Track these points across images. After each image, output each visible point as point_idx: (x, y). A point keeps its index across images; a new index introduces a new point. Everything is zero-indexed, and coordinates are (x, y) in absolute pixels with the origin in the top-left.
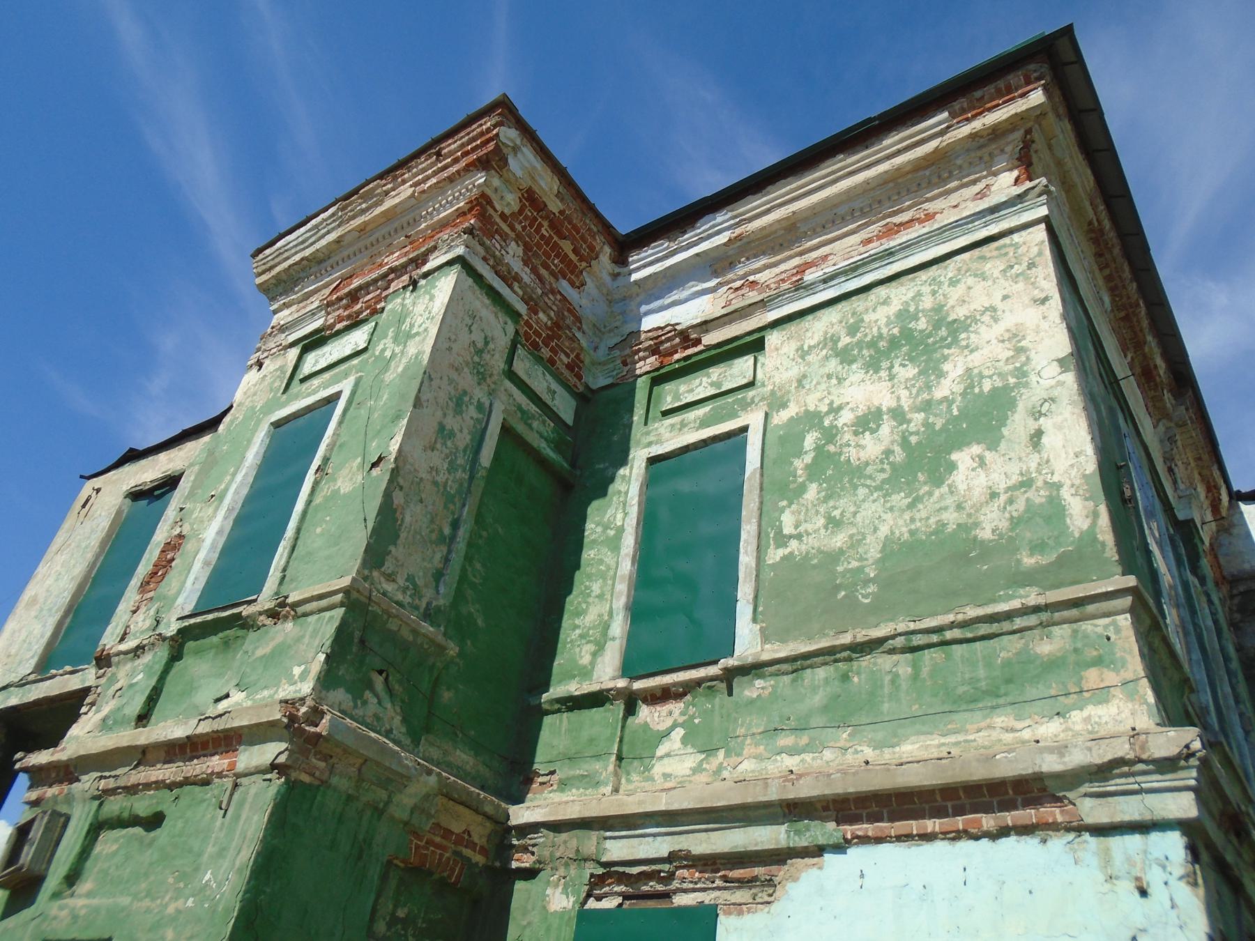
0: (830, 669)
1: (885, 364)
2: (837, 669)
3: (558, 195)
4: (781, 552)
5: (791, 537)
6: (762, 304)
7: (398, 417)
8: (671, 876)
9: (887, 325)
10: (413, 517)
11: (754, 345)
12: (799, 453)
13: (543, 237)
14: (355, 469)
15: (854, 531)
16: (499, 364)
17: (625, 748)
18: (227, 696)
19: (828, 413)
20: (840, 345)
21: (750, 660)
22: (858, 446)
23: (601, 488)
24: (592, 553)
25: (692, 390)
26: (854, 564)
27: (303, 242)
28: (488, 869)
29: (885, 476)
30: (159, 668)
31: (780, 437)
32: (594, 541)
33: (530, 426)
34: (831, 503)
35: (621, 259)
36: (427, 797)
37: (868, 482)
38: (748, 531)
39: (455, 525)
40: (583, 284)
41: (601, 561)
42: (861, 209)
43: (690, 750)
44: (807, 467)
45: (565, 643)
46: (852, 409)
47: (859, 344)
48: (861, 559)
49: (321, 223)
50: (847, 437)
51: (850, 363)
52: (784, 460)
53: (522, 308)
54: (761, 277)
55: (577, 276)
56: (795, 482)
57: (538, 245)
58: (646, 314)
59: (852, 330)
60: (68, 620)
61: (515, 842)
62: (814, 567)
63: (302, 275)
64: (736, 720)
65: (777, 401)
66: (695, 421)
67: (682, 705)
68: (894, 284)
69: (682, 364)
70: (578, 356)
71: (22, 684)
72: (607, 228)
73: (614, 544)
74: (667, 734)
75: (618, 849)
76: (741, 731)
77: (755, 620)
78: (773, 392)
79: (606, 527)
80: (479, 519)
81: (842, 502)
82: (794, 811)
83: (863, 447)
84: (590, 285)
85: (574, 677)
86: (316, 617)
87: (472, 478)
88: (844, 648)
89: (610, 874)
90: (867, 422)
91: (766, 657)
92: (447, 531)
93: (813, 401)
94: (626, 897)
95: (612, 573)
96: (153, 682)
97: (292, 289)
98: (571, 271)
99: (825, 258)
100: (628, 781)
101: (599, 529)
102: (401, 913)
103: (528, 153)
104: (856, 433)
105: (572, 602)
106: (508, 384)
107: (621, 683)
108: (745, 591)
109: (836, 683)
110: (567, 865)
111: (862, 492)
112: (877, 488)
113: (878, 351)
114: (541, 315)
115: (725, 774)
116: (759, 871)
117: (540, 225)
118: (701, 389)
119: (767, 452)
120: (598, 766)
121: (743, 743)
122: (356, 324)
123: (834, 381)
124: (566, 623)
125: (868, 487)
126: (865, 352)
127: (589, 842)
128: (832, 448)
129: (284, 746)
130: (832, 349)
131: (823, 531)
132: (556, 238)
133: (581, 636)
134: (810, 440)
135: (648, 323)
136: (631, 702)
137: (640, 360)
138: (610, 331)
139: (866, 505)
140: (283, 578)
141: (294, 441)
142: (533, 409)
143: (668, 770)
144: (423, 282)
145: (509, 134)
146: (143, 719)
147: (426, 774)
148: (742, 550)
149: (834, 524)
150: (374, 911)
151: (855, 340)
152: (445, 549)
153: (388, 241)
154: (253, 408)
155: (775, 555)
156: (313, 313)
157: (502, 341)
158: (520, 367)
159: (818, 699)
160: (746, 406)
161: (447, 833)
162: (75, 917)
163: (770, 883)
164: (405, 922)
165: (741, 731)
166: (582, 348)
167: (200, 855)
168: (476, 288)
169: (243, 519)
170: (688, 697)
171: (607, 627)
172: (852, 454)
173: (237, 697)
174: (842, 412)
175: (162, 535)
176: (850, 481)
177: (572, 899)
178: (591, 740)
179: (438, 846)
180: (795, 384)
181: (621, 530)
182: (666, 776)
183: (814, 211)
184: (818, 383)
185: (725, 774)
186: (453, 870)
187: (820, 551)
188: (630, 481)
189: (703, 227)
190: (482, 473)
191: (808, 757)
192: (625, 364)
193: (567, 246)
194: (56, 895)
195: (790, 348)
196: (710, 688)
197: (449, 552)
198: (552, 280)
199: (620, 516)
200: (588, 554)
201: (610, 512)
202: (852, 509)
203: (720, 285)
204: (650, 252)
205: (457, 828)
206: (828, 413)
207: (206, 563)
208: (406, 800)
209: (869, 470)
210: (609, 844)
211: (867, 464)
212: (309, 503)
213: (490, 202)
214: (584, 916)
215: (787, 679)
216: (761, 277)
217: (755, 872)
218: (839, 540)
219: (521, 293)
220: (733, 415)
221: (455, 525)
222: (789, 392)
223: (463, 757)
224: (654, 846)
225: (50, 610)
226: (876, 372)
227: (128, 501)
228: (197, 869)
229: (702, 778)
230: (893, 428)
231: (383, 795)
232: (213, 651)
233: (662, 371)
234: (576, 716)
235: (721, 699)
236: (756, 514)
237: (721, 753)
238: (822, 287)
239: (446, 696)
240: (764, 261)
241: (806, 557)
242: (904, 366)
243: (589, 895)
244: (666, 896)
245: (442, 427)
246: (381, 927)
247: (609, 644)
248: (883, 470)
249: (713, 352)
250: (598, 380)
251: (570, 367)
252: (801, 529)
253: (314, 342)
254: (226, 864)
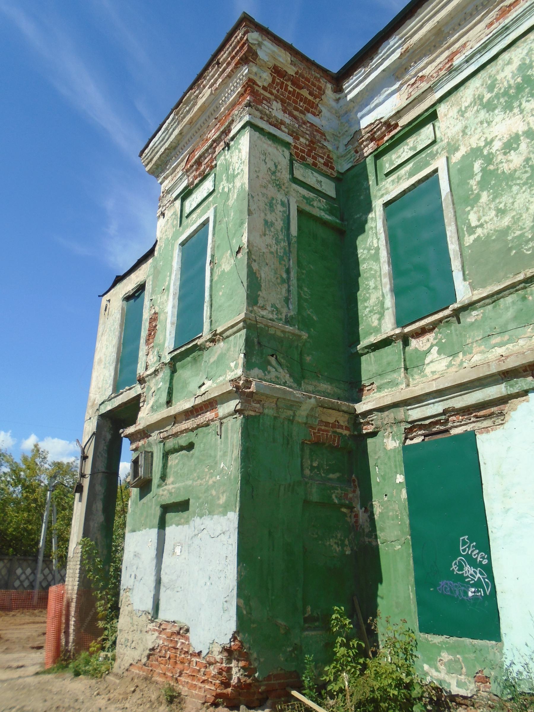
0: (514, 296)
1: (516, 104)
2: (518, 295)
3: (292, 63)
4: (472, 237)
5: (477, 227)
6: (431, 90)
7: (242, 223)
8: (447, 421)
9: (513, 77)
10: (265, 274)
11: (431, 116)
12: (472, 176)
13: (290, 92)
14: (229, 257)
15: (514, 213)
16: (286, 176)
17: (408, 363)
18: (204, 384)
19: (485, 146)
20: (485, 100)
21: (466, 302)
22: (508, 161)
23: (361, 229)
24: (365, 266)
25: (400, 156)
26: (518, 233)
27: (162, 140)
28: (352, 436)
29: (528, 175)
30: (168, 378)
31: (459, 170)
32: (364, 259)
33: (313, 205)
34: (497, 201)
35: (339, 89)
36: (312, 409)
37: (518, 182)
38: (450, 230)
39: (288, 272)
40: (320, 112)
41: (371, 269)
42: (482, 4)
43: (443, 356)
44: (479, 183)
45: (362, 317)
46: (500, 139)
47: (497, 96)
48: (522, 229)
49: (168, 126)
50: (500, 157)
51: (493, 110)
52: (464, 182)
53: (289, 139)
54: (426, 72)
55: (316, 108)
56: (472, 194)
57: (289, 98)
58: (362, 117)
59: (491, 88)
60: (119, 366)
61: (362, 421)
62: (494, 240)
63: (168, 159)
64: (465, 336)
65: (453, 148)
66: (405, 174)
67: (434, 334)
68: (513, 48)
69: (390, 142)
70: (328, 156)
71: (110, 399)
72: (325, 72)
73: (376, 257)
74: (429, 351)
75: (416, 413)
76: (469, 341)
77: (465, 279)
78: (448, 143)
79: (369, 250)
80: (299, 264)
81: (504, 199)
82: (507, 375)
83: (511, 161)
85: (371, 333)
86: (233, 337)
87: (289, 244)
88: (520, 282)
89: (414, 426)
90: (511, 144)
91: (475, 298)
92: (285, 276)
93: (475, 141)
94: (425, 436)
95: (378, 274)
96: (167, 385)
97: (166, 168)
98: (312, 107)
99: (464, 46)
100: (413, 379)
101: (365, 252)
102: (315, 464)
103: (268, 45)
104: (505, 154)
105: (361, 294)
106: (294, 186)
107: (398, 331)
108: (456, 265)
109: (519, 303)
110: (391, 426)
111: (515, 189)
112: (524, 184)
113: (510, 96)
114: (302, 140)
115: (465, 365)
116: (493, 409)
117: (287, 86)
118: (404, 154)
119: (452, 181)
120: (395, 375)
121: (472, 347)
122: (204, 178)
123: (485, 125)
124: (360, 306)
125: (518, 184)
126: (502, 100)
127: (400, 413)
128: (491, 167)
129: (237, 401)
130: (480, 105)
131: (495, 219)
132: (297, 90)
133: (370, 312)
134: (477, 166)
135: (364, 123)
136: (405, 340)
137: (365, 147)
138: (343, 134)
139: (519, 196)
140: (211, 321)
141: (194, 250)
142: (312, 195)
143: (434, 370)
144: (232, 143)
145: (254, 36)
146: (169, 403)
147: (309, 399)
148: (449, 242)
149: (501, 212)
150: (302, 466)
151: (494, 94)
152: (286, 286)
153: (206, 125)
154: (168, 238)
155: (469, 240)
156: (181, 179)
157: (284, 162)
158: (298, 173)
159: (510, 314)
160: (433, 156)
161: (327, 424)
162: (171, 493)
163: (501, 414)
164: (318, 468)
165: (469, 341)
166: (330, 151)
167: (215, 457)
168: (262, 136)
169: (182, 298)
170: (436, 330)
171: (382, 303)
172: (505, 167)
173: (208, 383)
174: (494, 143)
175: (146, 315)
176: (507, 184)
177: (398, 442)
178: (388, 364)
179: (323, 431)
180: (461, 134)
181: (378, 249)
182: (433, 373)
183: (451, 16)
184: (476, 129)
185: (465, 365)
186: (334, 441)
187: (496, 231)
188: (376, 219)
189: (383, 51)
190: (294, 240)
191: (510, 346)
192: (356, 152)
193: (305, 93)
194: (159, 486)
195: (454, 112)
196: (447, 322)
197: (289, 287)
198: (302, 116)
199: (375, 241)
200: (363, 267)
201: (369, 240)
202: (511, 201)
203: (402, 85)
204: (355, 78)
205: (331, 420)
206: (485, 146)
207: (172, 324)
208: (302, 413)
209: (517, 174)
210: (410, 412)
211: (515, 171)
212: (211, 281)
213: (255, 83)
214: (405, 449)
215: (490, 307)
216: (426, 72)
217: (492, 411)
218: (506, 221)
219: (286, 130)
220: (427, 164)
221: (288, 272)
222: (458, 140)
223: (325, 386)
224: (435, 408)
225: (109, 363)
226: (511, 110)
227: (125, 302)
228: (216, 463)
229: (453, 369)
230: (528, 144)
231: (291, 413)
232: (190, 364)
233: (379, 150)
234: (377, 353)
235: (455, 326)
236: (453, 219)
237: (461, 355)
238: (466, 66)
239: (308, 359)
240: (426, 60)
241: (488, 236)
242: (528, 101)
243: (406, 439)
244: (447, 431)
245: (266, 222)
246: (307, 472)
247: (386, 312)
248: (526, 172)
249: (407, 129)
250: (343, 166)
251: (325, 164)
252: (482, 221)
253: (186, 194)
254: (228, 458)
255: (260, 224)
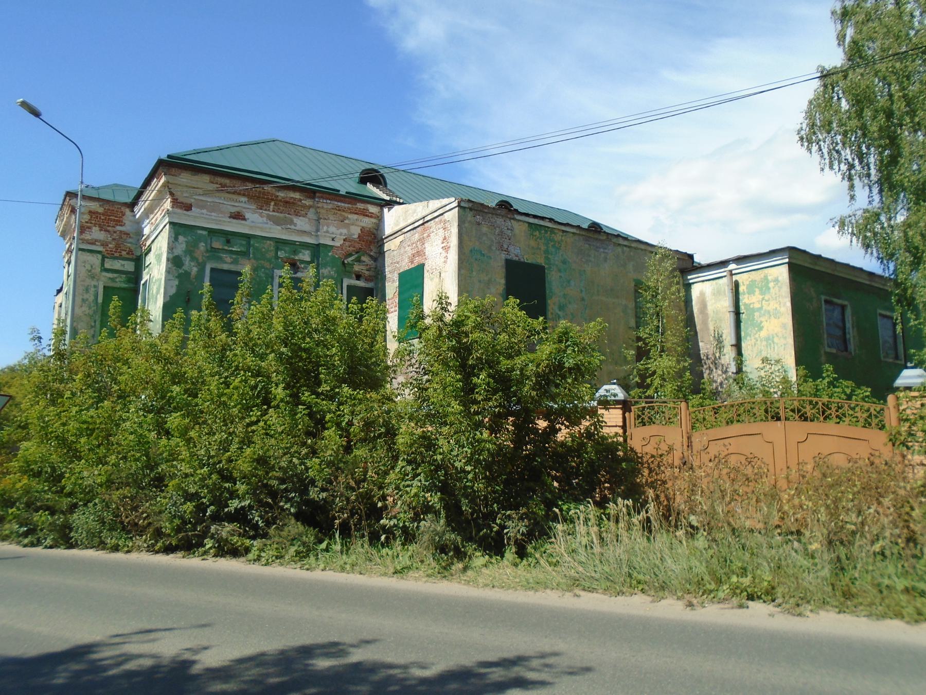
72: (125, 204)
84: (127, 223)
98: (120, 222)
106: (104, 274)
142: (116, 275)
158: (107, 266)
245: (83, 300)
255: (79, 300)
